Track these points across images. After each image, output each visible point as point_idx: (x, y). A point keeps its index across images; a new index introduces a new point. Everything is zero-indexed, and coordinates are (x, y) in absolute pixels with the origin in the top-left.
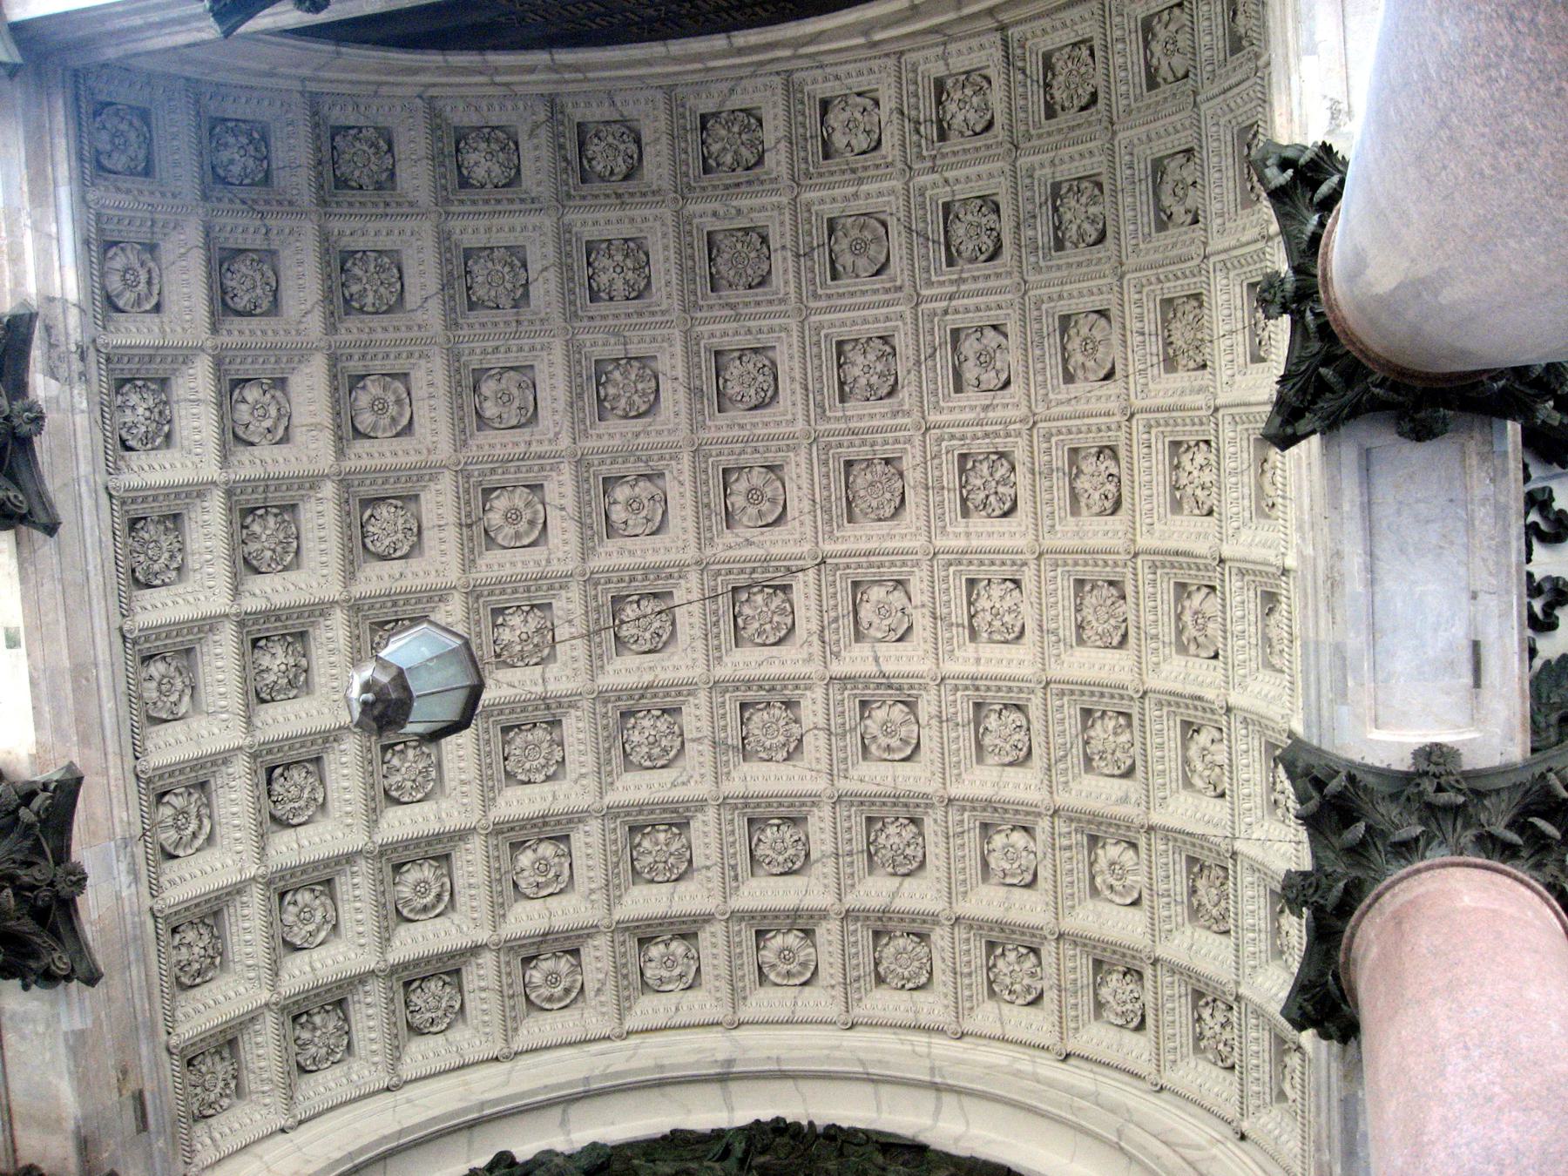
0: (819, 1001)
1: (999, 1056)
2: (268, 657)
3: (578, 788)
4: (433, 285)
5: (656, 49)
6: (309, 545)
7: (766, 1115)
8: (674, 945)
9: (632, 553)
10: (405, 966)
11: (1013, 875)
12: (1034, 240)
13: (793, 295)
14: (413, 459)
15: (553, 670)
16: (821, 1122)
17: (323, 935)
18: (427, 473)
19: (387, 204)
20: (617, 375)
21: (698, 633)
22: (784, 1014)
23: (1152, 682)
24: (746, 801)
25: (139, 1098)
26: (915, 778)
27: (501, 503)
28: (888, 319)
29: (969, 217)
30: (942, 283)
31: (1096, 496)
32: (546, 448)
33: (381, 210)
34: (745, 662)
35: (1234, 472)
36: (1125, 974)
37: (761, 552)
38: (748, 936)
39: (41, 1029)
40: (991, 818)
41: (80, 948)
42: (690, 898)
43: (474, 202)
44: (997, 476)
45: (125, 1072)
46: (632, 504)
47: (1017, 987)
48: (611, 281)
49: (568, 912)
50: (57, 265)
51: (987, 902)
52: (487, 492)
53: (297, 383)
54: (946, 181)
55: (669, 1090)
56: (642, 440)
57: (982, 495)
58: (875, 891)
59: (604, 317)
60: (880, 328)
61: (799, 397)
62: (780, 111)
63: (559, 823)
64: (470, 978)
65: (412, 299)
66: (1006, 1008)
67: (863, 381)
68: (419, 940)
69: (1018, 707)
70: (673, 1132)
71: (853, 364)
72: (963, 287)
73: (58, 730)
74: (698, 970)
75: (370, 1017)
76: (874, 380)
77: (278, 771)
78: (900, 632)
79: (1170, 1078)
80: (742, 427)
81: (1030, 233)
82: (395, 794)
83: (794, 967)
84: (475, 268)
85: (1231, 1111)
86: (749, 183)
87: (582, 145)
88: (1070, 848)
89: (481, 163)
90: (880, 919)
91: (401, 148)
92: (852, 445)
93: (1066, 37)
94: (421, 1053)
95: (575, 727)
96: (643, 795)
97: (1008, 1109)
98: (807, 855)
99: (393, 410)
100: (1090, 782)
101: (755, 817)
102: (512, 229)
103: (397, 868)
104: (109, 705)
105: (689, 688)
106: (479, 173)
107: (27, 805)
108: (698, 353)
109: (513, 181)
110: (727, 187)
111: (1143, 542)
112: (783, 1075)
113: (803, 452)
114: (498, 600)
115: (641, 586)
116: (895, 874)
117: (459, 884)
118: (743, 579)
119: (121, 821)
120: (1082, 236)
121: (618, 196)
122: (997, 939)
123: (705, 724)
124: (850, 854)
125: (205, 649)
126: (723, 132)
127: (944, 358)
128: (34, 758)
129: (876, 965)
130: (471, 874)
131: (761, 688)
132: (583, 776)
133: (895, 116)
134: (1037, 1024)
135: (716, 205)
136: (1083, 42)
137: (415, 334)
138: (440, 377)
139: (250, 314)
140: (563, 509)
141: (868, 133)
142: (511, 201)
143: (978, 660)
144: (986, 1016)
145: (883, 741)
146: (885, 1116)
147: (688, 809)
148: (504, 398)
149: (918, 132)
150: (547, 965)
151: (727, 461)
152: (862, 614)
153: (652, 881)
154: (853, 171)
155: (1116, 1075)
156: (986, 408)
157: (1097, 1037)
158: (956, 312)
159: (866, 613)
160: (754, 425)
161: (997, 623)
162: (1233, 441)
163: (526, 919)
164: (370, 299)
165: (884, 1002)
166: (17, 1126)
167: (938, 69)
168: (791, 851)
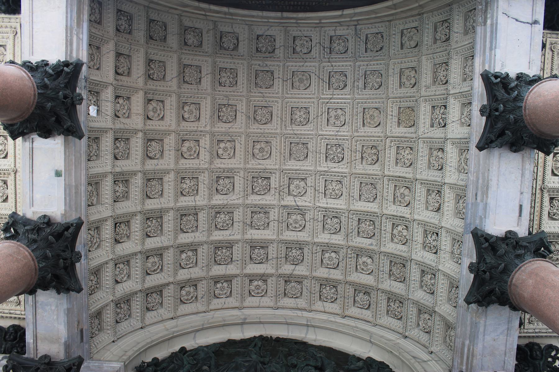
0: (267, 301)
1: (324, 317)
2: (118, 187)
3: (202, 235)
4: (175, 74)
5: (260, 13)
6: (133, 151)
7: (257, 334)
8: (224, 284)
9: (224, 164)
10: (148, 289)
11: (331, 265)
12: (358, 86)
13: (281, 92)
14: (164, 128)
15: (197, 198)
16: (274, 337)
17: (125, 278)
18: (167, 133)
19: (164, 47)
20: (224, 109)
21: (241, 189)
22: (257, 304)
23: (385, 212)
24: (252, 241)
25: (82, 331)
26: (303, 236)
27: (187, 144)
28: (309, 103)
29: (337, 77)
30: (327, 94)
31: (370, 159)
32: (202, 129)
33: (162, 48)
34: (254, 199)
35: (422, 156)
36: (364, 294)
37: (263, 167)
38: (247, 281)
39: (53, 308)
40: (326, 248)
41: (77, 281)
42: (232, 269)
43: (189, 50)
44: (338, 151)
45: (79, 322)
46: (225, 150)
47: (329, 297)
48: (226, 81)
49: (196, 272)
50: (81, 49)
51: (322, 273)
52: (184, 141)
53: (134, 99)
54: (332, 66)
55: (225, 327)
56: (231, 130)
57: (332, 156)
58: (287, 269)
59: (223, 91)
60: (306, 105)
61: (279, 123)
62: (282, 37)
63: (195, 245)
64: (165, 293)
65: (168, 78)
66: (325, 303)
67: (299, 120)
68: (153, 280)
69: (337, 217)
70: (229, 340)
71: (296, 114)
72: (334, 96)
73: (70, 207)
74: (231, 291)
75: (137, 305)
76: (302, 120)
77: (118, 224)
78: (302, 194)
79: (379, 322)
80: (261, 129)
81: (358, 84)
82: (149, 234)
83: (260, 291)
84: (186, 71)
85: (401, 331)
86: (271, 57)
87: (221, 38)
88: (351, 258)
89: (191, 39)
90: (288, 277)
91: (169, 30)
92: (294, 138)
93: (375, 30)
94: (151, 316)
95: (202, 216)
96: (221, 238)
97: (330, 332)
98: (267, 257)
99: (159, 112)
100: (359, 240)
101: (254, 245)
102: (199, 61)
103: (148, 257)
104: (83, 199)
105: (237, 206)
106: (190, 42)
107: (67, 231)
108: (250, 106)
109: (201, 45)
110: (264, 58)
111: (386, 173)
112: (260, 323)
113: (278, 138)
114: (184, 175)
115: (226, 174)
116: (293, 264)
117: (165, 263)
118: (256, 175)
119: (84, 238)
120: (373, 86)
121: (231, 55)
122: (324, 283)
123: (241, 218)
124: (281, 258)
125: (103, 183)
126: (263, 41)
127: (325, 116)
128: (64, 215)
129: (285, 290)
130: (169, 260)
131: (259, 207)
132: (203, 231)
133: (318, 45)
134: (334, 307)
135: (260, 63)
136: (380, 33)
137: (168, 88)
138: (174, 104)
139: (122, 75)
140: (205, 148)
141: (308, 48)
142: (200, 52)
143: (327, 203)
144: (319, 305)
145: (294, 225)
146: (290, 334)
147: (233, 243)
148: (191, 112)
149: (324, 50)
150: (187, 289)
151: (255, 139)
152: (291, 188)
153: (220, 264)
154: (303, 59)
155: (361, 321)
156: (337, 131)
157: (354, 311)
158: (331, 103)
159: (292, 187)
160: (265, 129)
161: (333, 193)
162: (422, 148)
163: (183, 275)
164: (155, 76)
165: (288, 302)
166: (39, 342)
167: (332, 33)
168: (262, 257)
